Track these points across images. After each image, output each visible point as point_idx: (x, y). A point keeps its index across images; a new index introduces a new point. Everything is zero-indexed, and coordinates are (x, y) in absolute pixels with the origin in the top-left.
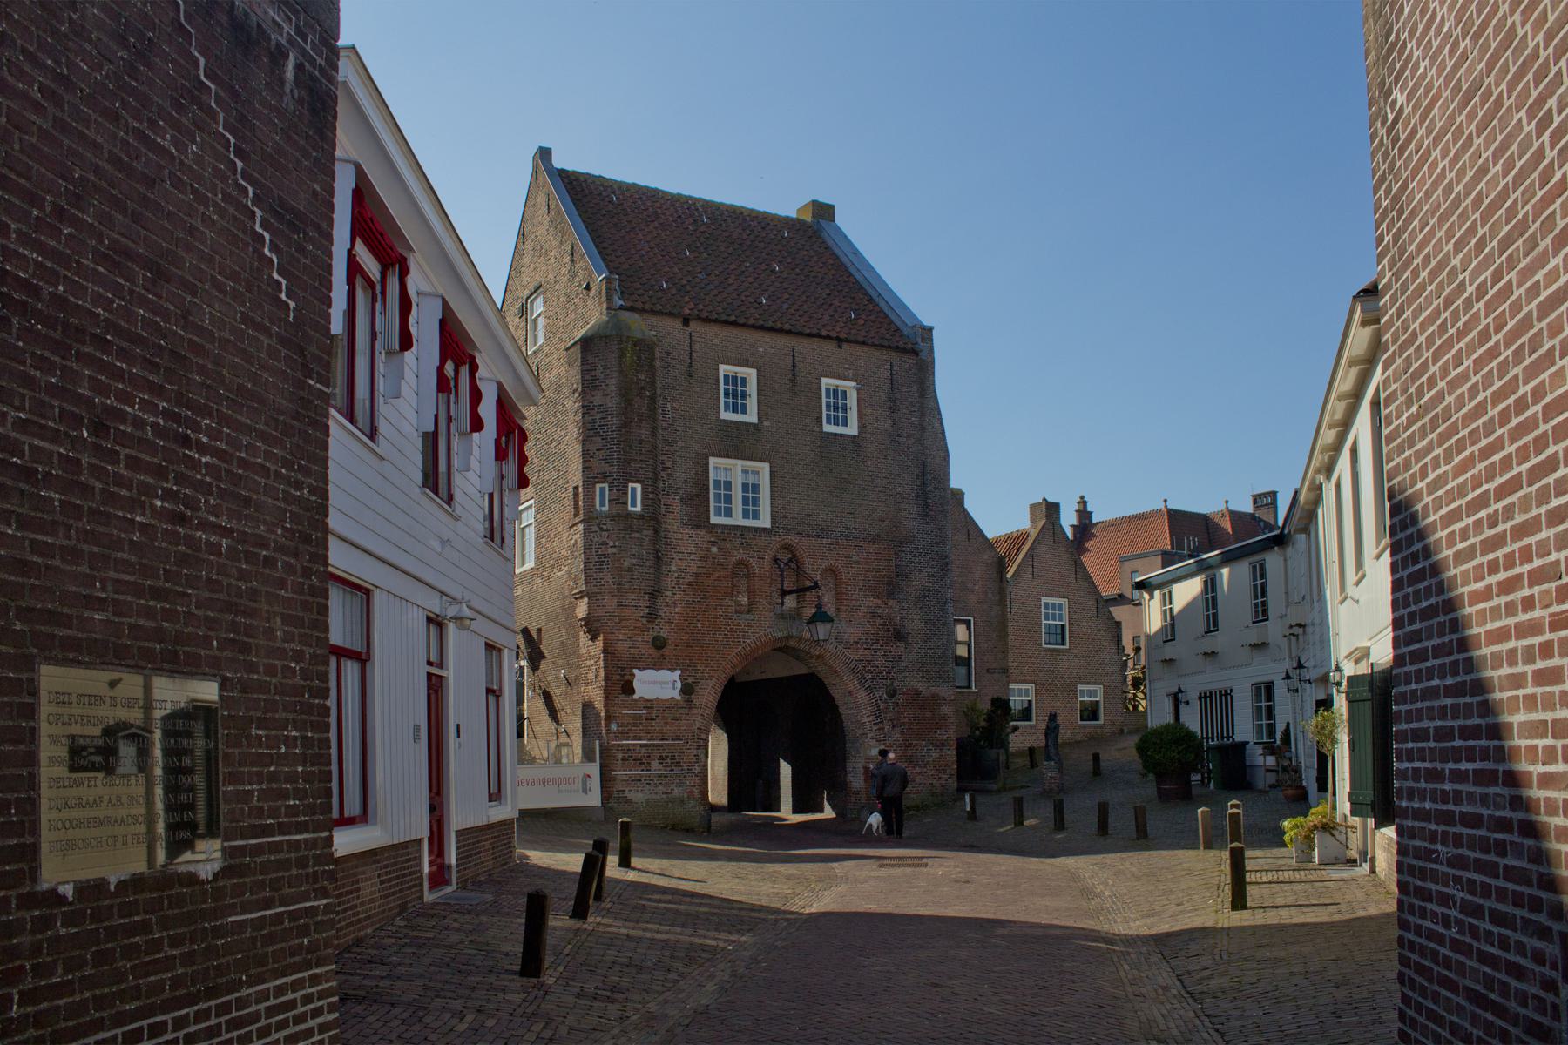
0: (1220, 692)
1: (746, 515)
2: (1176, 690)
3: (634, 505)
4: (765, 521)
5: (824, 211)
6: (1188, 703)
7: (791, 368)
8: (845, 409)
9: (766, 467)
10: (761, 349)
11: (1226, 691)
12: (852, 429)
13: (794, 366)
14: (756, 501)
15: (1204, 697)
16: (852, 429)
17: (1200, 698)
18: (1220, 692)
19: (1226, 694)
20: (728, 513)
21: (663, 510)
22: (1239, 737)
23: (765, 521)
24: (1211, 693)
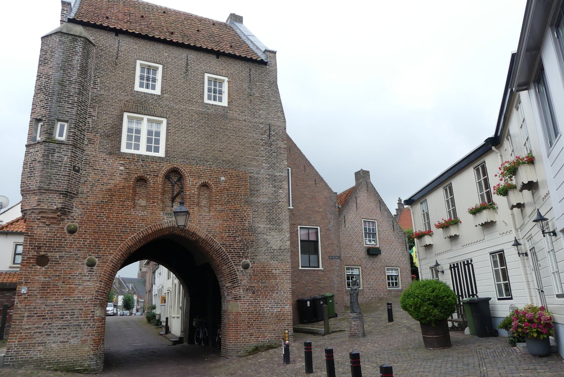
0: (464, 262)
1: (149, 149)
2: (434, 264)
3: (61, 135)
4: (162, 153)
5: (236, 18)
6: (443, 272)
7: (185, 65)
8: (221, 92)
9: (165, 121)
10: (166, 54)
11: (468, 261)
12: (225, 103)
13: (187, 64)
14: (157, 142)
15: (454, 267)
16: (225, 103)
17: (451, 268)
18: (464, 262)
19: (468, 264)
20: (137, 147)
21: (86, 142)
22: (481, 295)
23: (162, 153)
24: (457, 264)
